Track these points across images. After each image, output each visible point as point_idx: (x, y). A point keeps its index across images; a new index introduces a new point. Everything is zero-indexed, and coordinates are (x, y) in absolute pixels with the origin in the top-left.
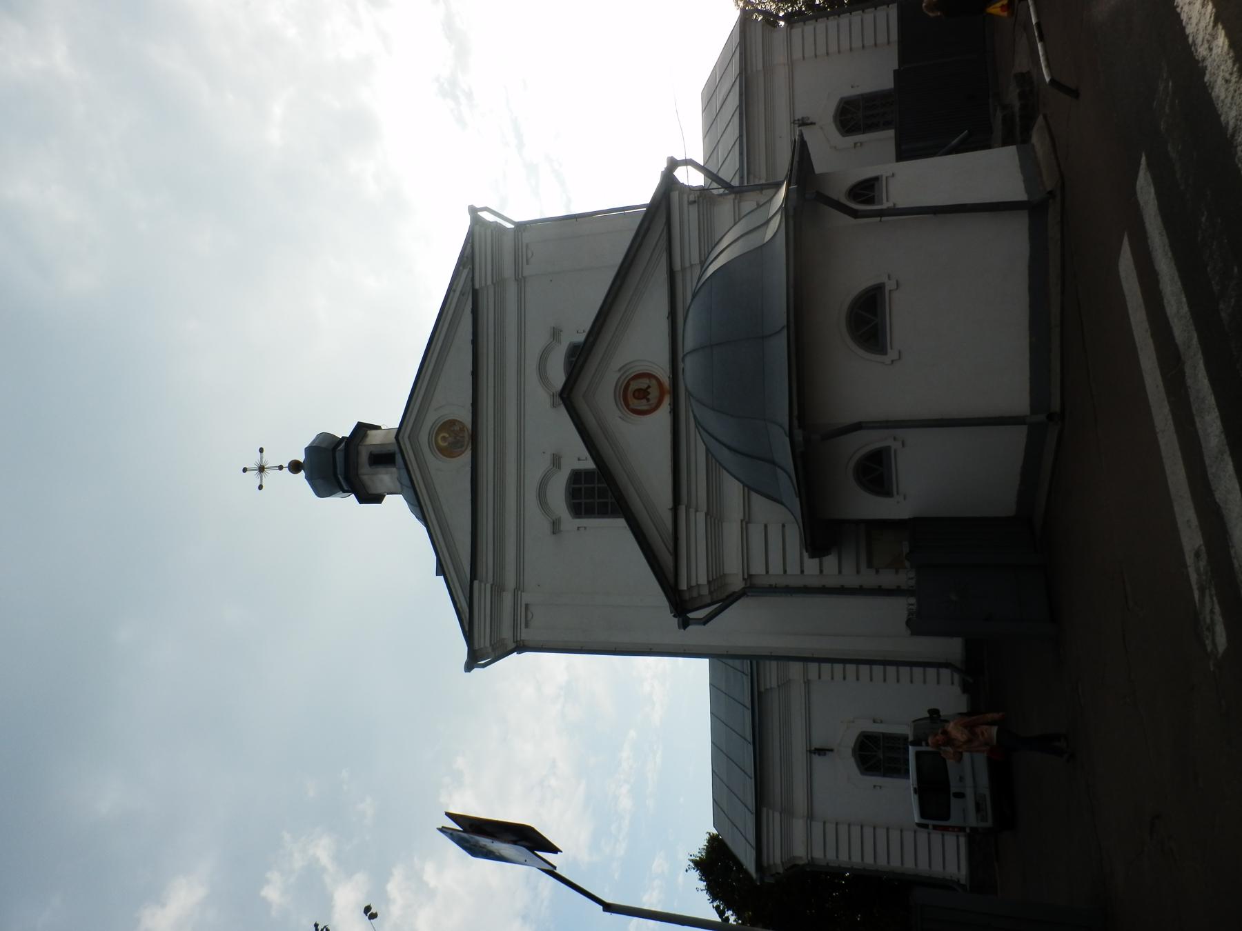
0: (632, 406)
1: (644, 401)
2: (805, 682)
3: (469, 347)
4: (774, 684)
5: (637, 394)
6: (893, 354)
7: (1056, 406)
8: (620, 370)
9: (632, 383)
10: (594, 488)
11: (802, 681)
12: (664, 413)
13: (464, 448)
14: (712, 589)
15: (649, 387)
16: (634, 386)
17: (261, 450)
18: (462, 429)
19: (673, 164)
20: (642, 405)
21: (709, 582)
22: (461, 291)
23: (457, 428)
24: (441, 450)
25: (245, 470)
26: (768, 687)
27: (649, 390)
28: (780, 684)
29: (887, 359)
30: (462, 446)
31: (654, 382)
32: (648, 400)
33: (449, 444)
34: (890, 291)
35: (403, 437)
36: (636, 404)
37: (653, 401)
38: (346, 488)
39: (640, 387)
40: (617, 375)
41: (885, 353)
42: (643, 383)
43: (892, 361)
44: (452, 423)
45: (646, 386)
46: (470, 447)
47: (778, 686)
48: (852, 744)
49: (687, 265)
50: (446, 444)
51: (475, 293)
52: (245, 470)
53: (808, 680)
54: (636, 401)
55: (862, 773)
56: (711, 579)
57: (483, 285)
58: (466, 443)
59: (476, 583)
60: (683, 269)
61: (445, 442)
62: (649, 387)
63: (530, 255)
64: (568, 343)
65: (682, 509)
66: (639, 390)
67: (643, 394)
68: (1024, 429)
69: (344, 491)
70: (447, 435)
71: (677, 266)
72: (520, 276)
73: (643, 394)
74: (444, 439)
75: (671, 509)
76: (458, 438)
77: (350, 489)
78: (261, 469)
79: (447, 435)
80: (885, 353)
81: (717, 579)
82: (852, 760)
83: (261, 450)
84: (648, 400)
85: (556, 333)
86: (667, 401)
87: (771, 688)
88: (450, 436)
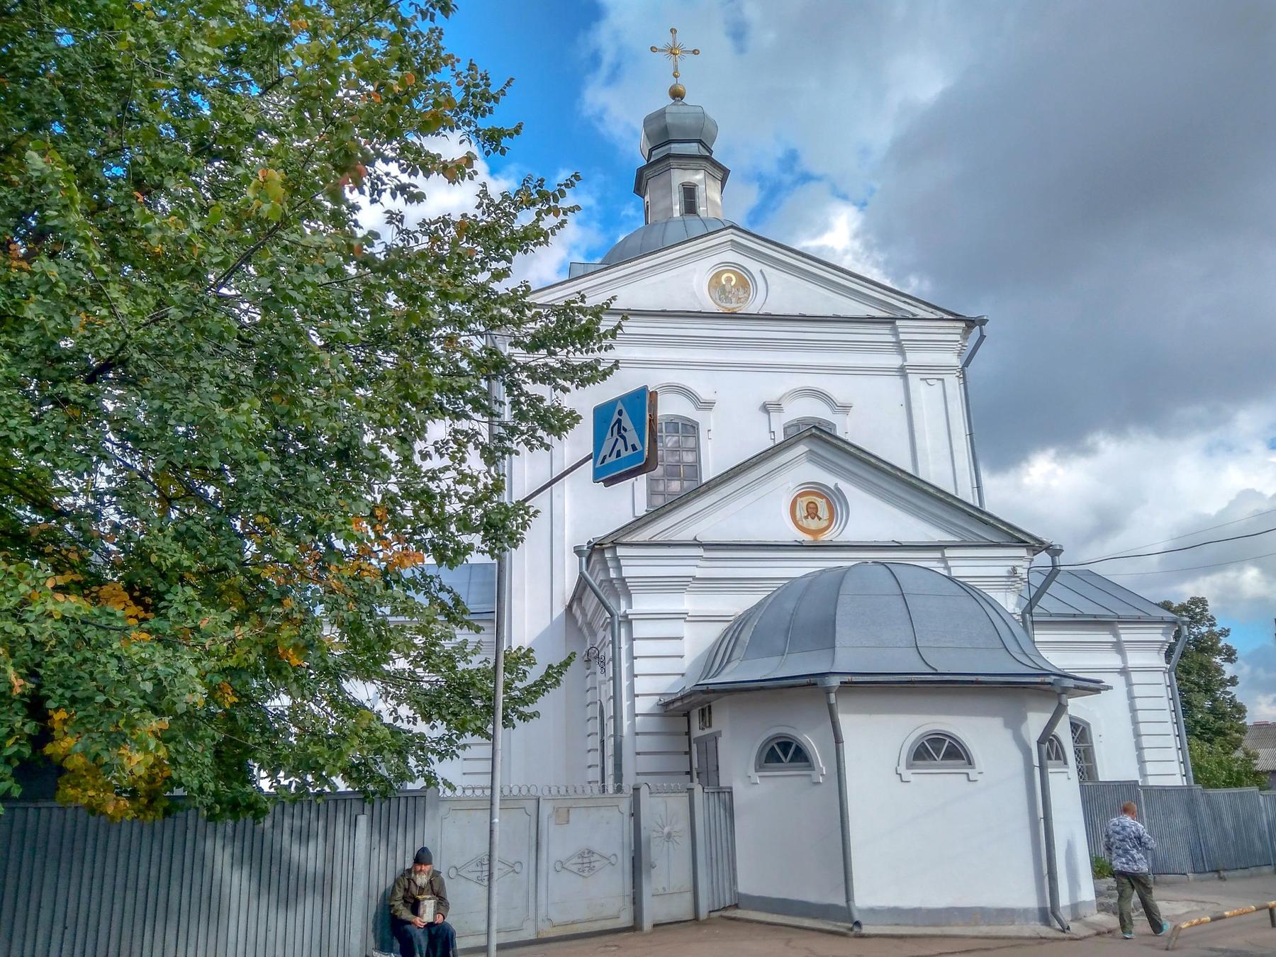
0: (799, 500)
5: (811, 505)
6: (907, 774)
9: (824, 500)
12: (791, 533)
13: (718, 301)
15: (820, 519)
16: (821, 504)
17: (695, 52)
19: (1054, 552)
20: (801, 512)
23: (741, 294)
24: (718, 276)
25: (673, 31)
29: (902, 769)
31: (825, 524)
32: (806, 517)
36: (802, 503)
37: (805, 523)
41: (909, 766)
42: (823, 511)
52: (673, 31)
54: (805, 504)
58: (724, 304)
62: (820, 519)
65: (699, 552)
66: (817, 508)
67: (812, 512)
69: (651, 151)
70: (733, 283)
71: (948, 553)
73: (812, 512)
74: (729, 280)
75: (695, 539)
77: (652, 160)
79: (733, 283)
80: (909, 766)
81: (622, 588)
83: (695, 52)
84: (806, 517)
85: (845, 408)
86: (807, 538)
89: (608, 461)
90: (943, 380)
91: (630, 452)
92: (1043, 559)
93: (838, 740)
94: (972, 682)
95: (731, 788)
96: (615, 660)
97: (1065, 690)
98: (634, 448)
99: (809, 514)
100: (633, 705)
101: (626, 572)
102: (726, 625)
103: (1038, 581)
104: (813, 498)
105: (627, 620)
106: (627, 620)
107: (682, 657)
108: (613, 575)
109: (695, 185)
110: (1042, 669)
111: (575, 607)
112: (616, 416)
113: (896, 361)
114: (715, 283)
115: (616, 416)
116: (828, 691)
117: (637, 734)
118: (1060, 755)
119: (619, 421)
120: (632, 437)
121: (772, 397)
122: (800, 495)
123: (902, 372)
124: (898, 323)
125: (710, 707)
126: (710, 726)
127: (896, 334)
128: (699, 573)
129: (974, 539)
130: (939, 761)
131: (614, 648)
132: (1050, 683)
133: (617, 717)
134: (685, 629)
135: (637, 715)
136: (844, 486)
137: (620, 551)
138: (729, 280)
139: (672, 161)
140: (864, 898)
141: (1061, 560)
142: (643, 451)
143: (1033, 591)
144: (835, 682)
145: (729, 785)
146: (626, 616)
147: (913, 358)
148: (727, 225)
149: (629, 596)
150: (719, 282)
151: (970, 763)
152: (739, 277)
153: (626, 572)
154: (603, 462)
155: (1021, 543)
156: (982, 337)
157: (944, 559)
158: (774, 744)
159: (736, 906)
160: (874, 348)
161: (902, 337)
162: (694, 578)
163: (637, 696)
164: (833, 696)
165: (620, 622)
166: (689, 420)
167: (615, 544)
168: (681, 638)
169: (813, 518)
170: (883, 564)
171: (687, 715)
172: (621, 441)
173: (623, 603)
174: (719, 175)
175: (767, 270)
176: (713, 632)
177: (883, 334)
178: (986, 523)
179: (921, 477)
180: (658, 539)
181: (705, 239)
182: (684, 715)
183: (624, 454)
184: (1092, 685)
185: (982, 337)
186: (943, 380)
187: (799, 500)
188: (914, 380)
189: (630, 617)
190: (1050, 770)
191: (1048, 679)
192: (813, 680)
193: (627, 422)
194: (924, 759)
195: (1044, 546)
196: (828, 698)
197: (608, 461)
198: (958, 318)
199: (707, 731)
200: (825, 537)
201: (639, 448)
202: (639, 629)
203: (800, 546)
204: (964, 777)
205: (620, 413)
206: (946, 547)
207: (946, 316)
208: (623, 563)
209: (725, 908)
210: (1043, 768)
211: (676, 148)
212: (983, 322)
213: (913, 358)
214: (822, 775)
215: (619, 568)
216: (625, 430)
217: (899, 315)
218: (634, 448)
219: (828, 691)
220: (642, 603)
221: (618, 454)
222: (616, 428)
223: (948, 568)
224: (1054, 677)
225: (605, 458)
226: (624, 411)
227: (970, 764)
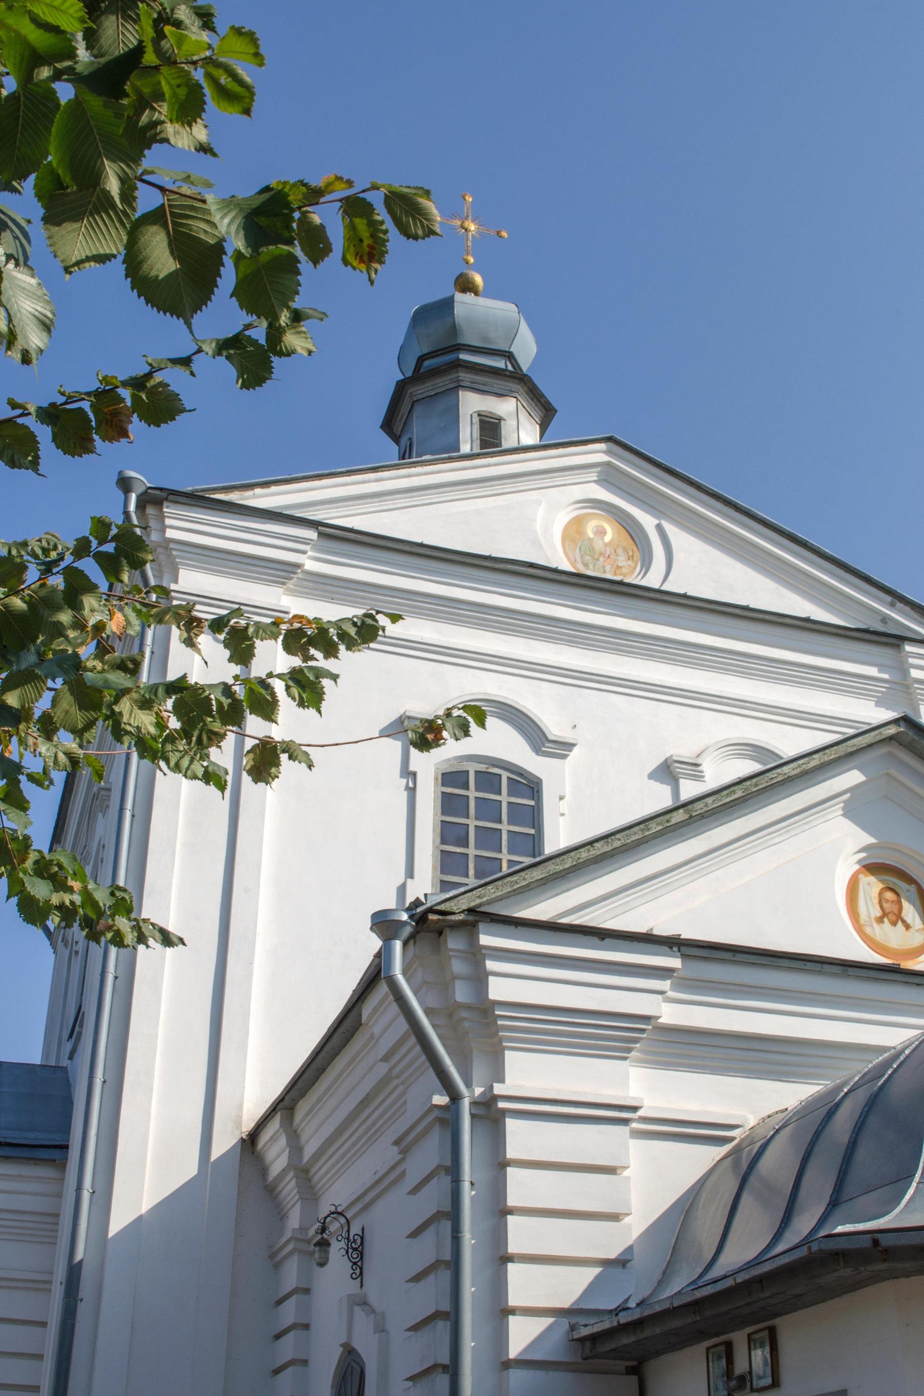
15: (908, 927)
27: (900, 923)
32: (880, 920)
33: (591, 540)
38: (426, 363)
50: (591, 534)
61: (595, 533)
62: (908, 927)
70: (608, 538)
76: (601, 559)
79: (608, 538)
84: (880, 920)
88: (606, 545)
99: (885, 914)
100: (501, 1337)
101: (498, 990)
108: (462, 993)
109: (500, 419)
121: (683, 750)
124: (908, 648)
127: (903, 670)
135: (507, 1364)
138: (601, 532)
139: (465, 376)
150: (581, 532)
153: (498, 990)
168: (611, 1170)
169: (894, 924)
173: (479, 1071)
181: (561, 451)
182: (631, 1371)
189: (501, 1105)
215: (480, 979)
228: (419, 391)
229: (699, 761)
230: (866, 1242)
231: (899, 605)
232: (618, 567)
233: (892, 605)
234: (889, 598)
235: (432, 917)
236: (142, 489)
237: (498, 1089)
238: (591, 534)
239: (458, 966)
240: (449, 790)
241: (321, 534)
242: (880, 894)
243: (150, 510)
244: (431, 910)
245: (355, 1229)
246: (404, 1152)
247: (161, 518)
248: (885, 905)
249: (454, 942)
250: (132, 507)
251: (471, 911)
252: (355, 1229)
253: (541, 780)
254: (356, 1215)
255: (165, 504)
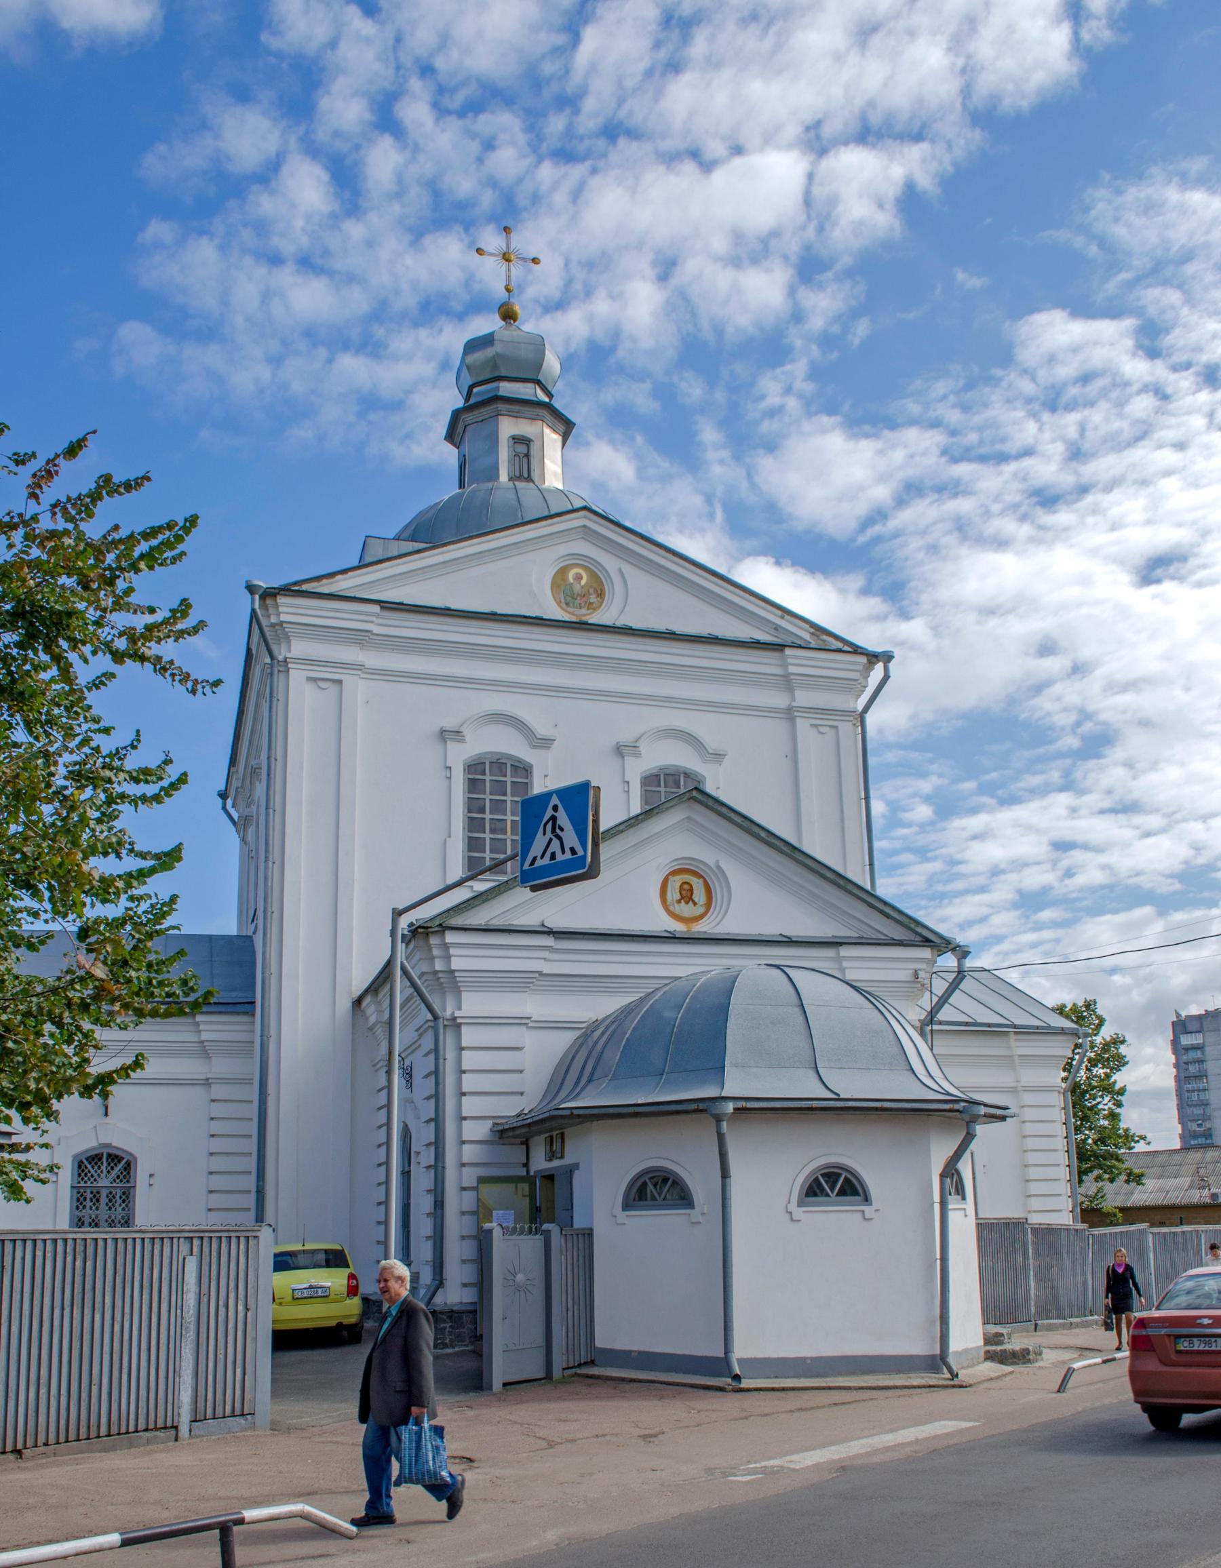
0: (671, 878)
1: (678, 897)
2: (208, 1079)
3: (703, 631)
4: (204, 1036)
5: (686, 887)
6: (798, 1212)
7: (745, 1383)
8: (719, 868)
9: (701, 881)
10: (505, 794)
11: (209, 1076)
12: (663, 923)
13: (564, 606)
14: (440, 975)
15: (695, 904)
16: (697, 884)
18: (591, 607)
19: (962, 953)
20: (673, 894)
21: (453, 972)
22: (780, 626)
23: (593, 598)
24: (563, 571)
26: (202, 1027)
28: (206, 1044)
29: (793, 1206)
30: (567, 604)
31: (701, 910)
32: (679, 902)
34: (863, 1211)
35: (585, 517)
36: (675, 883)
38: (475, 390)
39: (695, 892)
40: (711, 863)
41: (799, 1206)
42: (699, 895)
43: (791, 1213)
44: (601, 594)
45: (696, 900)
46: (567, 617)
47: (202, 1042)
48: (115, 1143)
49: (845, 964)
50: (571, 580)
51: (779, 647)
53: (209, 1085)
54: (678, 884)
55: (75, 1157)
56: (457, 974)
57: (789, 661)
58: (571, 610)
59: (376, 609)
60: (839, 959)
61: (575, 579)
62: (695, 904)
63: (821, 729)
64: (704, 773)
65: (549, 941)
66: (691, 890)
67: (687, 895)
68: (722, 1355)
70: (583, 582)
71: (844, 951)
72: (796, 714)
74: (578, 577)
75: (543, 925)
77: (472, 401)
78: (506, 257)
79: (583, 582)
80: (801, 1204)
81: (451, 982)
82: (94, 1144)
84: (679, 902)
85: (718, 757)
86: (678, 927)
87: (200, 1031)
88: (582, 587)
89: (539, 863)
90: (836, 727)
91: (568, 855)
92: (949, 961)
93: (725, 1175)
94: (876, 1109)
95: (591, 1230)
96: (436, 1074)
97: (974, 1119)
98: (573, 851)
99: (682, 898)
101: (456, 964)
102: (577, 1034)
103: (940, 987)
104: (687, 878)
105: (455, 1025)
106: (455, 1025)
107: (521, 1071)
108: (439, 965)
110: (948, 1094)
111: (367, 1001)
112: (549, 812)
113: (779, 700)
114: (559, 581)
115: (549, 812)
116: (718, 1119)
117: (463, 1165)
118: (960, 1190)
119: (554, 818)
120: (570, 838)
121: (626, 736)
122: (674, 873)
123: (790, 714)
124: (788, 651)
125: (562, 1135)
126: (562, 1157)
127: (785, 666)
128: (547, 968)
129: (869, 934)
130: (833, 1195)
131: (437, 1059)
132: (958, 1111)
133: (438, 1144)
134: (528, 1039)
136: (728, 866)
137: (450, 937)
138: (578, 577)
139: (501, 406)
140: (742, 1350)
141: (969, 963)
142: (584, 857)
143: (935, 999)
144: (730, 1107)
145: (589, 1226)
146: (454, 1019)
147: (803, 698)
148: (578, 504)
149: (458, 992)
150: (565, 579)
151: (867, 1200)
152: (593, 575)
154: (532, 863)
155: (926, 942)
156: (886, 677)
157: (839, 959)
158: (646, 1178)
159: (592, 1363)
160: (757, 681)
161: (792, 669)
162: (541, 974)
163: (465, 1118)
164: (725, 1123)
165: (445, 1026)
166: (520, 761)
167: (443, 928)
169: (687, 903)
170: (778, 967)
171: (526, 1143)
172: (556, 842)
174: (562, 428)
175: (628, 570)
176: (562, 1041)
177: (765, 663)
178: (887, 916)
179: (806, 849)
180: (497, 923)
181: (550, 521)
182: (522, 1143)
183: (560, 857)
184: (999, 1112)
185: (886, 677)
186: (836, 727)
187: (671, 878)
188: (802, 725)
189: (459, 1021)
190: (950, 1207)
191: (956, 1106)
192: (701, 1106)
193: (563, 819)
194: (815, 1195)
195: (950, 947)
196: (719, 1127)
197: (539, 863)
198: (857, 650)
199: (556, 1163)
200: (701, 927)
201: (580, 852)
202: (469, 1036)
203: (672, 938)
204: (859, 1215)
205: (555, 808)
206: (841, 944)
207: (846, 648)
208: (452, 951)
209: (580, 1365)
210: (943, 1203)
211: (506, 388)
212: (887, 657)
213: (803, 698)
214: (703, 1214)
215: (448, 958)
216: (562, 829)
217: (789, 640)
218: (573, 851)
219: (718, 1119)
220: (472, 1004)
221: (553, 856)
222: (549, 826)
223: (843, 970)
224: (963, 1104)
225: (535, 859)
226: (561, 808)
227: (866, 1200)
228: (468, 417)
229: (637, 744)
230: (567, 1112)
231: (787, 617)
232: (590, 603)
233: (782, 617)
234: (780, 613)
235: (420, 930)
236: (262, 590)
237: (457, 1014)
238: (571, 580)
239: (435, 952)
240: (470, 776)
241: (382, 608)
242: (681, 886)
243: (269, 601)
244: (419, 927)
245: (407, 1063)
246: (420, 1036)
247: (277, 606)
248: (683, 892)
249: (434, 940)
250: (257, 606)
251: (440, 925)
252: (407, 1063)
253: (531, 766)
254: (407, 1056)
255: (278, 597)
